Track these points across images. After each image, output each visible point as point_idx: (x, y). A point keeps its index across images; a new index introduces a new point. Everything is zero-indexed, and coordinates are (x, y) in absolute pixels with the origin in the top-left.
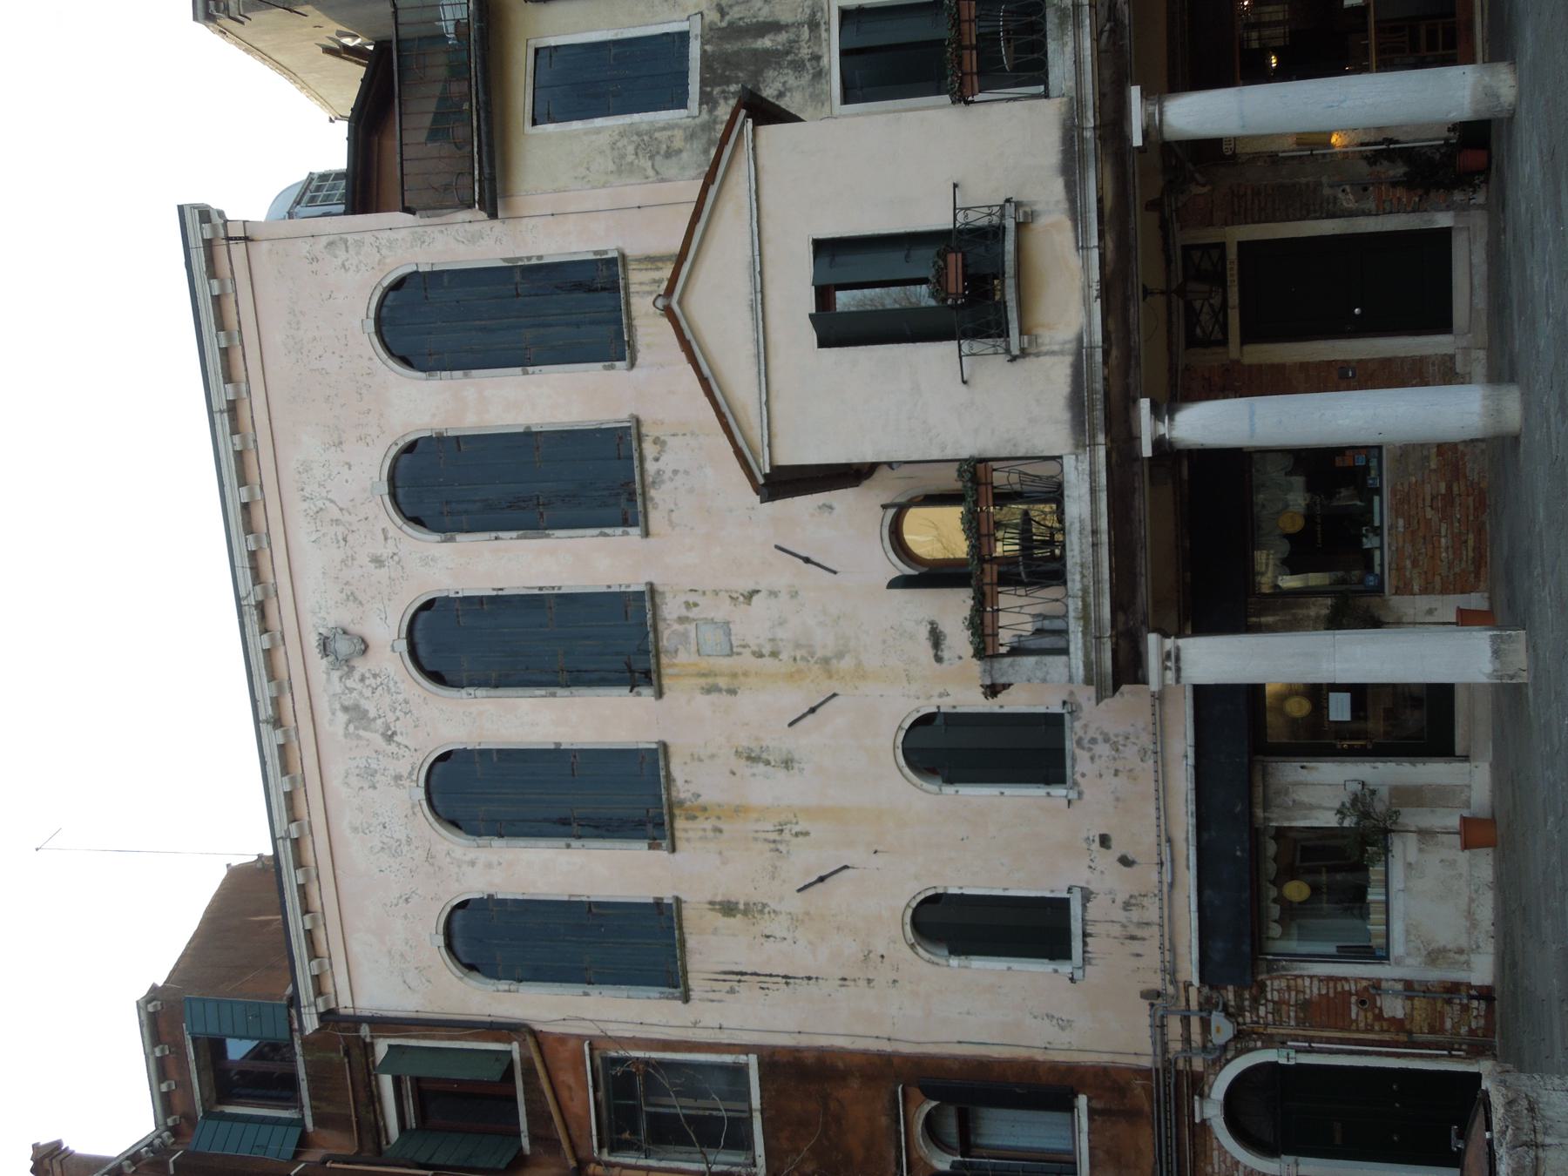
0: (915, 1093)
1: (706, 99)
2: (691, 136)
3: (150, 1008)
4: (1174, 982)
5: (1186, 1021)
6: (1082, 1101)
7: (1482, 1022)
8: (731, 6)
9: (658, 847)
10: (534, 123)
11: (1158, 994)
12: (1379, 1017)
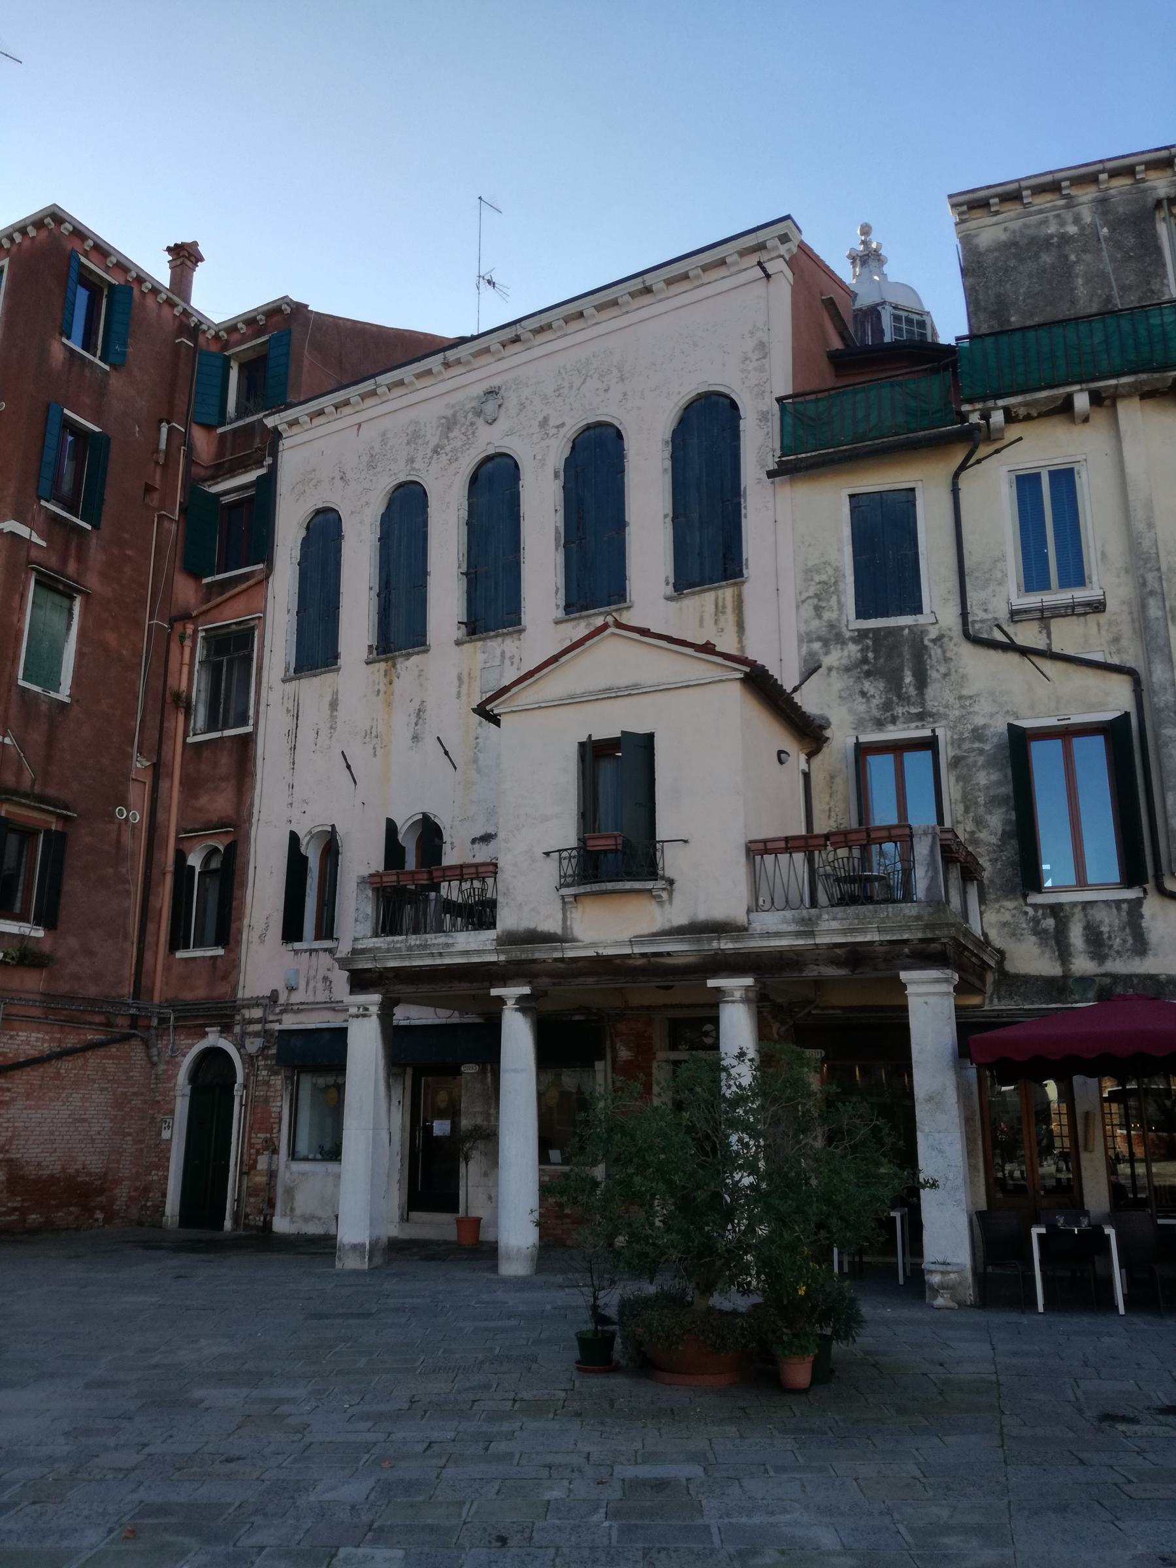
0: (227, 840)
1: (863, 634)
2: (832, 626)
3: (284, 307)
4: (282, 1012)
5: (258, 1021)
6: (220, 952)
7: (252, 1223)
8: (941, 647)
9: (370, 652)
10: (851, 496)
11: (275, 1002)
12: (258, 1153)
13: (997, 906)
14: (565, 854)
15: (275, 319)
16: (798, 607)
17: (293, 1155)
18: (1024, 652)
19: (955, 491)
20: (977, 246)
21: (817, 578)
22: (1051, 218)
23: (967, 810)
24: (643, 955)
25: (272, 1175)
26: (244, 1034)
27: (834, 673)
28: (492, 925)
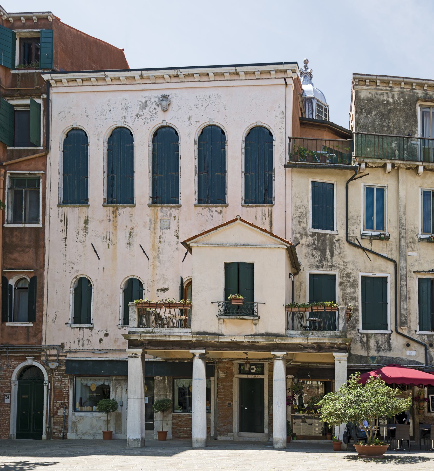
1: (314, 234)
2: (304, 229)
6: (31, 325)
8: (339, 243)
9: (105, 201)
12: (58, 408)
13: (350, 332)
14: (220, 304)
15: (43, 22)
16: (292, 220)
17: (75, 410)
18: (364, 249)
19: (347, 188)
20: (360, 97)
21: (299, 210)
22: (385, 94)
23: (343, 300)
24: (249, 342)
25: (66, 417)
26: (47, 360)
27: (304, 246)
28: (190, 327)
